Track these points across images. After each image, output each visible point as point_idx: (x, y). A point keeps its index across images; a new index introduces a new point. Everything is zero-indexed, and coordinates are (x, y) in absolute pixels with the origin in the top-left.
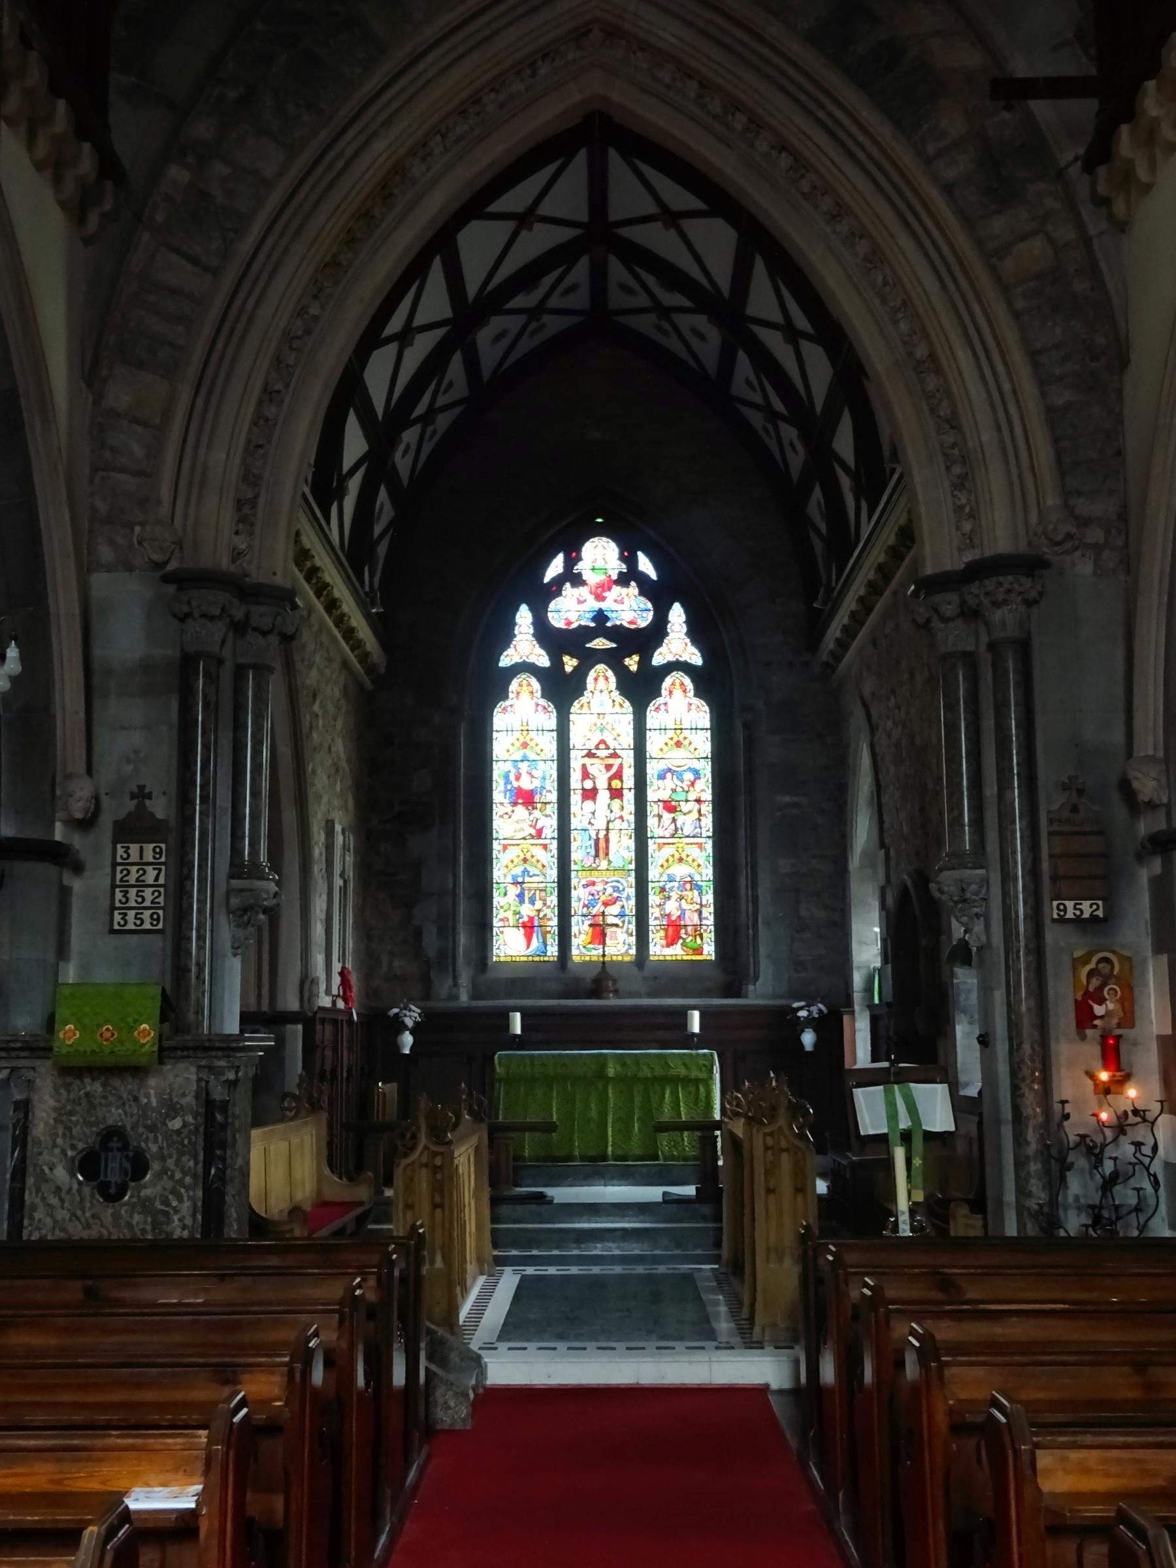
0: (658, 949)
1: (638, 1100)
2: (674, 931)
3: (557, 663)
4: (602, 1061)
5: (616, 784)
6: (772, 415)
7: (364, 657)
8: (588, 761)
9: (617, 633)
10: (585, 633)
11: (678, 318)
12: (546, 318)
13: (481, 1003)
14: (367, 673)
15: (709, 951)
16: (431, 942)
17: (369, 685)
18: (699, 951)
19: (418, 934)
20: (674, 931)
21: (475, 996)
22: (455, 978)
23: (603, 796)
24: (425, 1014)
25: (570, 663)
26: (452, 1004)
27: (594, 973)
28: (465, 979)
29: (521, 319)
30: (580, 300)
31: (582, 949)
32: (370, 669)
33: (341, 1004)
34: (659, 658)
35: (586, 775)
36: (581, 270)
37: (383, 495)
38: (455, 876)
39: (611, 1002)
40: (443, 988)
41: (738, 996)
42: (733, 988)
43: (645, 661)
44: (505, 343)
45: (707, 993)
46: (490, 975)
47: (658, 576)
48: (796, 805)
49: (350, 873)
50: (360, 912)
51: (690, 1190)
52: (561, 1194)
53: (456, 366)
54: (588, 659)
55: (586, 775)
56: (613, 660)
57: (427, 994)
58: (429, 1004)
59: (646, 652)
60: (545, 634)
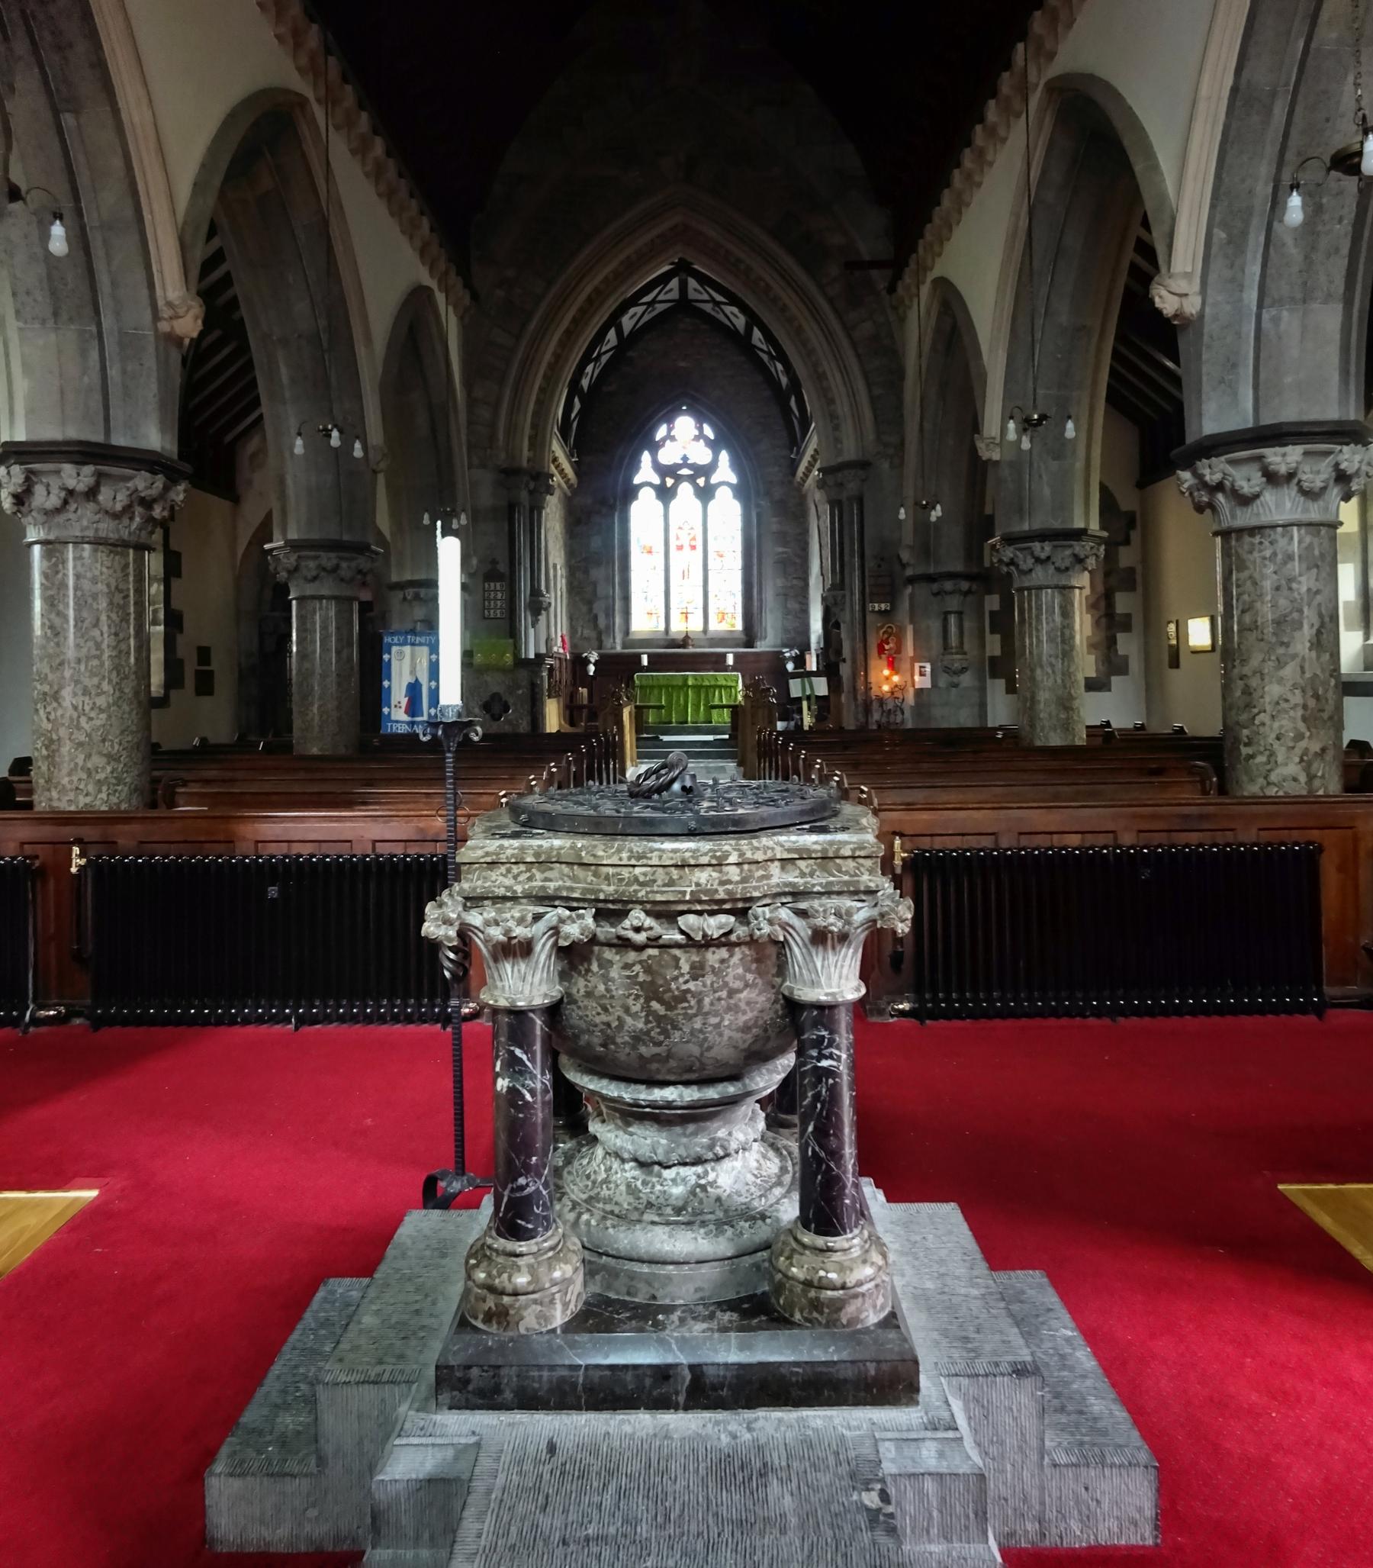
0: (715, 626)
1: (703, 697)
2: (723, 617)
3: (664, 482)
4: (686, 678)
5: (693, 543)
6: (771, 357)
7: (567, 482)
8: (680, 532)
9: (692, 467)
10: (679, 467)
11: (723, 307)
12: (657, 305)
13: (626, 651)
14: (569, 487)
15: (739, 626)
16: (602, 622)
17: (569, 494)
18: (733, 626)
19: (596, 617)
20: (723, 617)
21: (624, 646)
22: (614, 638)
23: (687, 548)
24: (600, 655)
25: (670, 482)
26: (613, 651)
27: (682, 636)
28: (618, 640)
29: (645, 307)
30: (675, 295)
31: (678, 627)
32: (570, 486)
33: (561, 651)
34: (714, 479)
35: (678, 538)
36: (674, 283)
37: (576, 400)
38: (614, 588)
39: (691, 650)
40: (608, 643)
41: (752, 647)
42: (749, 644)
43: (707, 481)
44: (635, 319)
45: (737, 646)
46: (631, 637)
47: (716, 436)
48: (783, 553)
49: (564, 588)
50: (568, 605)
51: (727, 737)
52: (666, 738)
53: (612, 335)
54: (679, 479)
55: (678, 538)
56: (692, 479)
57: (600, 647)
58: (602, 651)
59: (708, 476)
60: (659, 468)
